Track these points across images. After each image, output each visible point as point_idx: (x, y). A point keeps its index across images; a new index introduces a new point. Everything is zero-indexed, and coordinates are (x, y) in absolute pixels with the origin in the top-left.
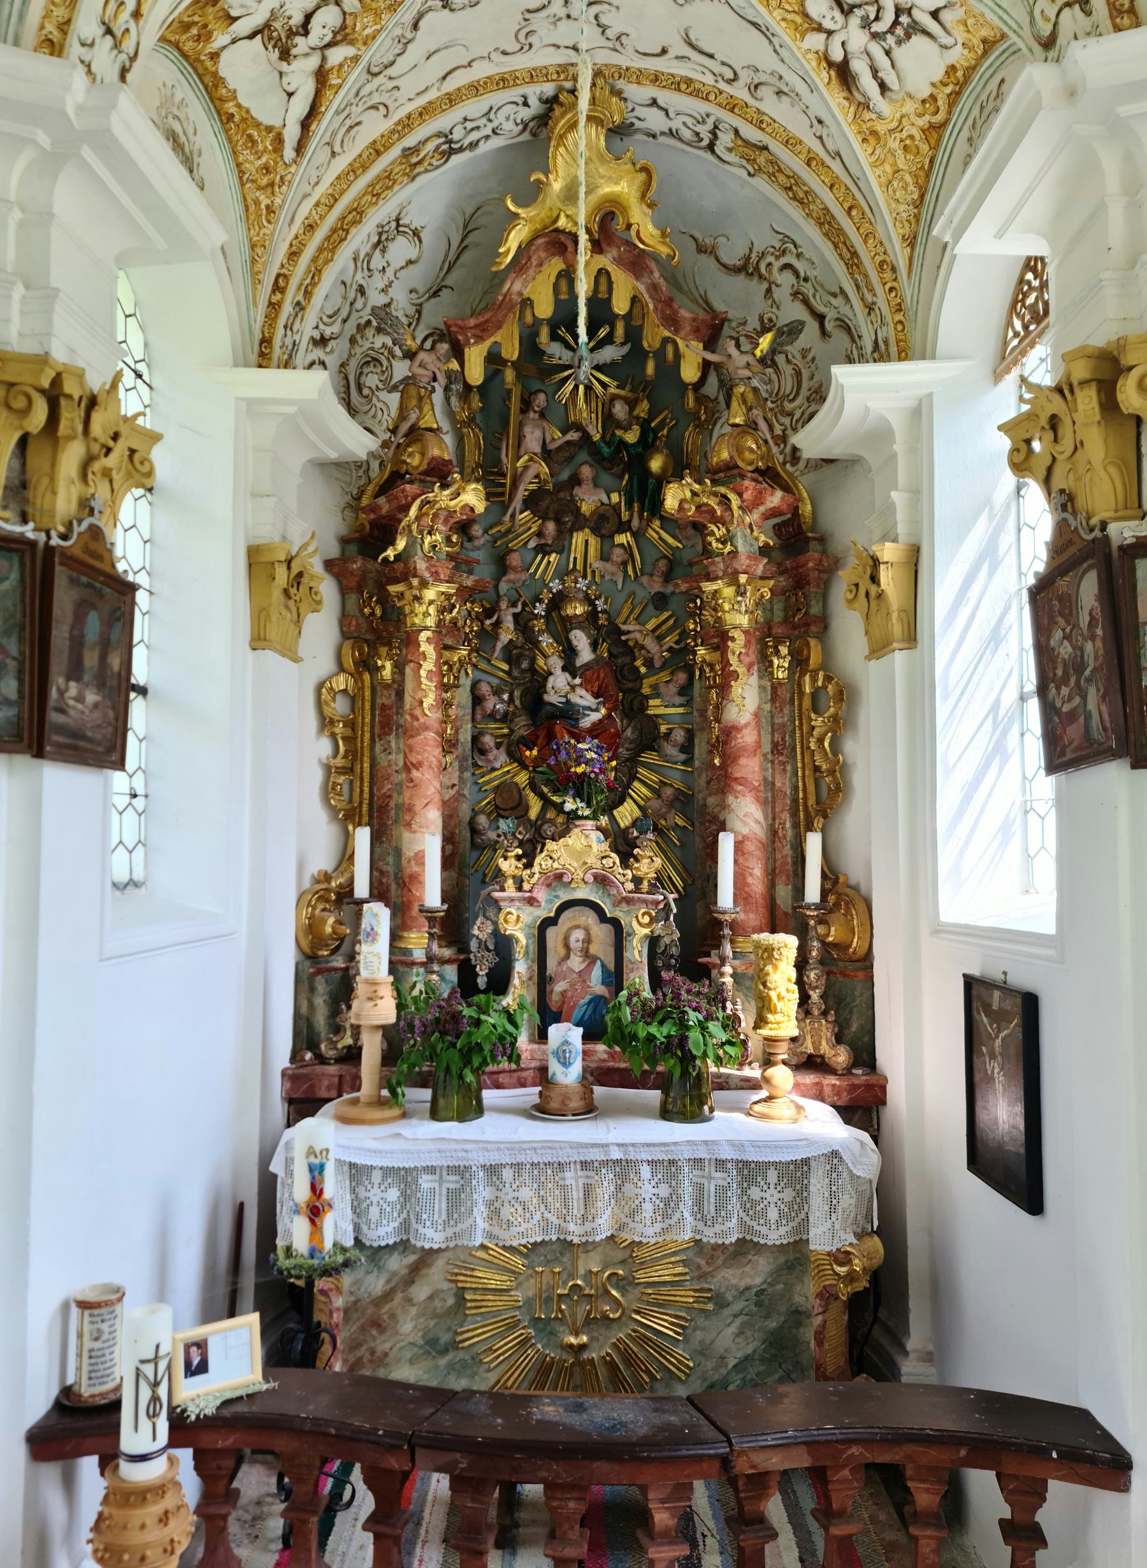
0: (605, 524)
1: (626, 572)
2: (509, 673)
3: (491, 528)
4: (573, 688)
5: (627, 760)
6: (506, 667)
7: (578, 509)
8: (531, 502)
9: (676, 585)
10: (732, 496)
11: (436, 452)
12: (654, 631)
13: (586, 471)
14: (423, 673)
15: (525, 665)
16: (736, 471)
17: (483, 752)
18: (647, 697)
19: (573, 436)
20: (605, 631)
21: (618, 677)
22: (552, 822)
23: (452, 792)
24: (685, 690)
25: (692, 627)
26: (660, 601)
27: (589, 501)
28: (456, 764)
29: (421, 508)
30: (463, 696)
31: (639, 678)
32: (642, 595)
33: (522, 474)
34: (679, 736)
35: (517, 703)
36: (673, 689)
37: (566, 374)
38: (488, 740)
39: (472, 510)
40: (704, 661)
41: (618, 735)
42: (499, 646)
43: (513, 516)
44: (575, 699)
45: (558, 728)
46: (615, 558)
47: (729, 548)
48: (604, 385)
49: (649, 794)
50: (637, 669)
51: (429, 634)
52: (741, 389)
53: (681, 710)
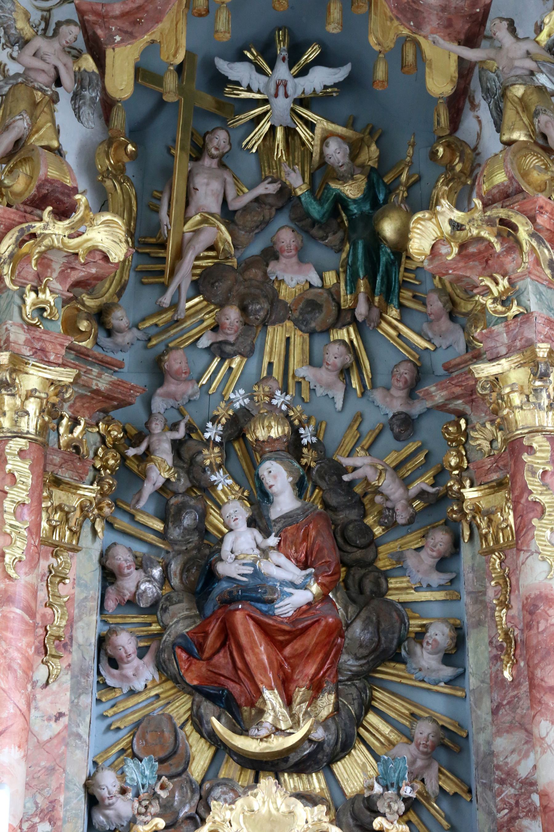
0: (317, 314)
1: (348, 385)
2: (163, 535)
3: (144, 320)
4: (265, 552)
5: (355, 676)
6: (159, 526)
7: (276, 293)
8: (202, 283)
9: (429, 395)
10: (518, 220)
11: (53, 173)
12: (396, 468)
13: (287, 238)
14: (8, 506)
15: (188, 520)
16: (520, 196)
17: (114, 663)
18: (386, 575)
19: (267, 188)
20: (320, 474)
21: (343, 536)
22: (228, 783)
23: (57, 727)
24: (446, 562)
25: (453, 461)
26: (405, 426)
27: (293, 279)
28: (66, 679)
29: (20, 243)
30: (83, 569)
31: (373, 543)
32: (373, 420)
33: (190, 240)
34: (439, 634)
35: (175, 581)
36: (428, 559)
37: (258, 111)
38: (125, 642)
39: (106, 258)
40: (477, 510)
41: (338, 630)
42: (148, 488)
43: (175, 305)
44: (267, 568)
45: (239, 617)
46: (331, 359)
47: (515, 309)
48: (311, 126)
49: (393, 737)
50: (368, 530)
51: (22, 443)
52: (519, 91)
53: (440, 595)
